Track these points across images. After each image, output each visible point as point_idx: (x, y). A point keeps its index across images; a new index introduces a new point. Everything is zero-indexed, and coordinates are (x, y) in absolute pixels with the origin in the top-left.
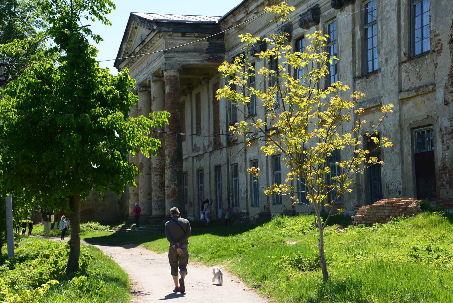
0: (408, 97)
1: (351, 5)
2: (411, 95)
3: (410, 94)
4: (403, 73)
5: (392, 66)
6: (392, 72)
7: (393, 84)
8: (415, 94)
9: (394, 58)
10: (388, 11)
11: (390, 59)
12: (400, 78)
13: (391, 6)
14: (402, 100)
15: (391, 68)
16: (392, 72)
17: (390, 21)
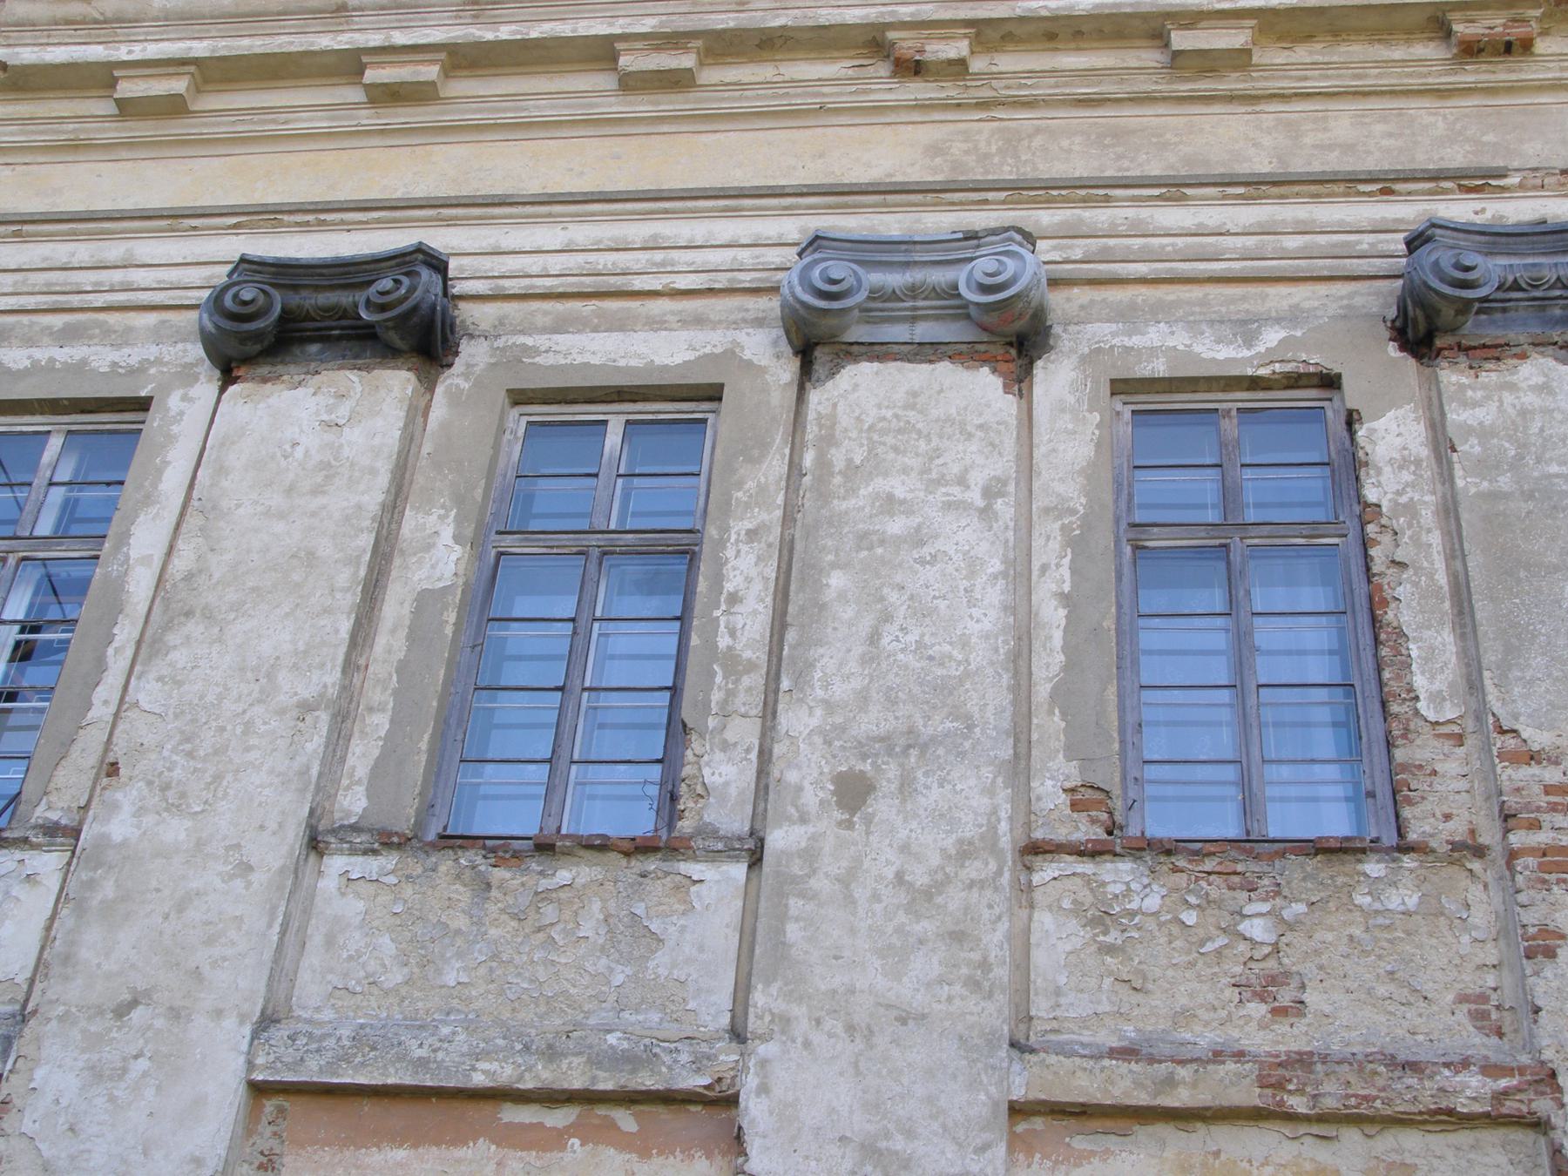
0: (1142, 1099)
1: (410, 375)
2: (1181, 1098)
3: (1170, 1082)
4: (1044, 920)
5: (934, 843)
6: (919, 877)
7: (926, 965)
8: (1248, 1095)
9: (970, 798)
10: (889, 504)
11: (906, 787)
12: (1022, 945)
13: (941, 481)
14: (1018, 1110)
15: (905, 849)
16: (919, 877)
17: (922, 562)
